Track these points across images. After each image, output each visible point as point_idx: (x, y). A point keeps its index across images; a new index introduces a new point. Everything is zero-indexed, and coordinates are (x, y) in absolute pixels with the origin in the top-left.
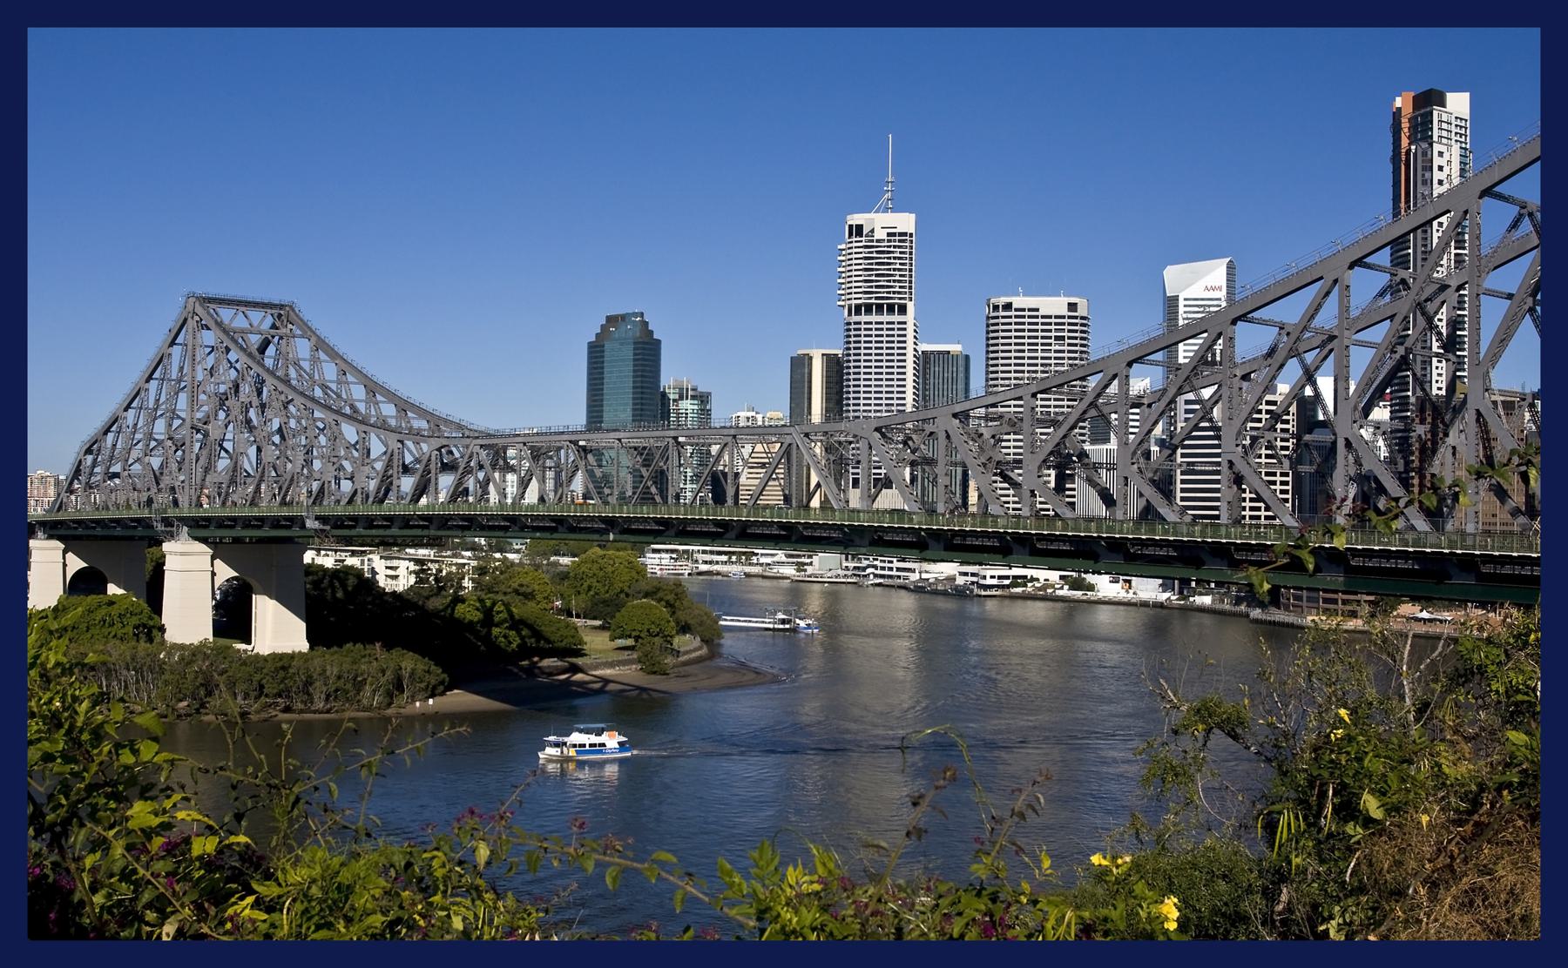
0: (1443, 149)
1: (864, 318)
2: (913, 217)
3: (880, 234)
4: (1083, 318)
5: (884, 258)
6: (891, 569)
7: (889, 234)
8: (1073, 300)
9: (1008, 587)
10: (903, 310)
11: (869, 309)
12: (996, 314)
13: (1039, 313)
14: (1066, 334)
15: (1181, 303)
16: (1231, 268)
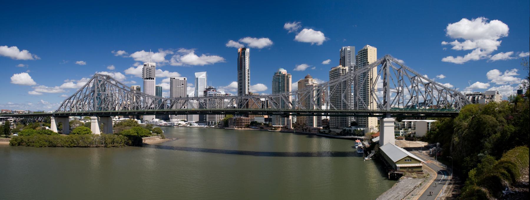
1: (147, 80)
3: (150, 66)
6: (154, 123)
8: (185, 78)
9: (178, 125)
10: (153, 79)
11: (148, 79)
13: (180, 80)
15: (199, 79)
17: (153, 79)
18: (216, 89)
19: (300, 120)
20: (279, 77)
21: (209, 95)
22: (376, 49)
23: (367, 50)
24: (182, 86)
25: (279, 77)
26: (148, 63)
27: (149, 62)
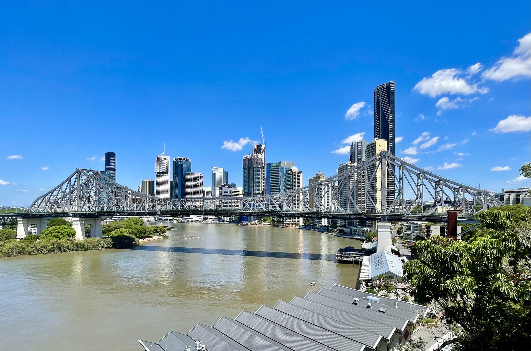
2: (169, 157)
3: (164, 160)
4: (202, 177)
7: (165, 160)
10: (167, 173)
11: (161, 173)
13: (195, 175)
14: (199, 179)
15: (216, 174)
17: (167, 173)
20: (290, 175)
21: (224, 191)
22: (387, 141)
23: (375, 143)
24: (197, 181)
25: (290, 175)
26: (161, 156)
27: (162, 155)
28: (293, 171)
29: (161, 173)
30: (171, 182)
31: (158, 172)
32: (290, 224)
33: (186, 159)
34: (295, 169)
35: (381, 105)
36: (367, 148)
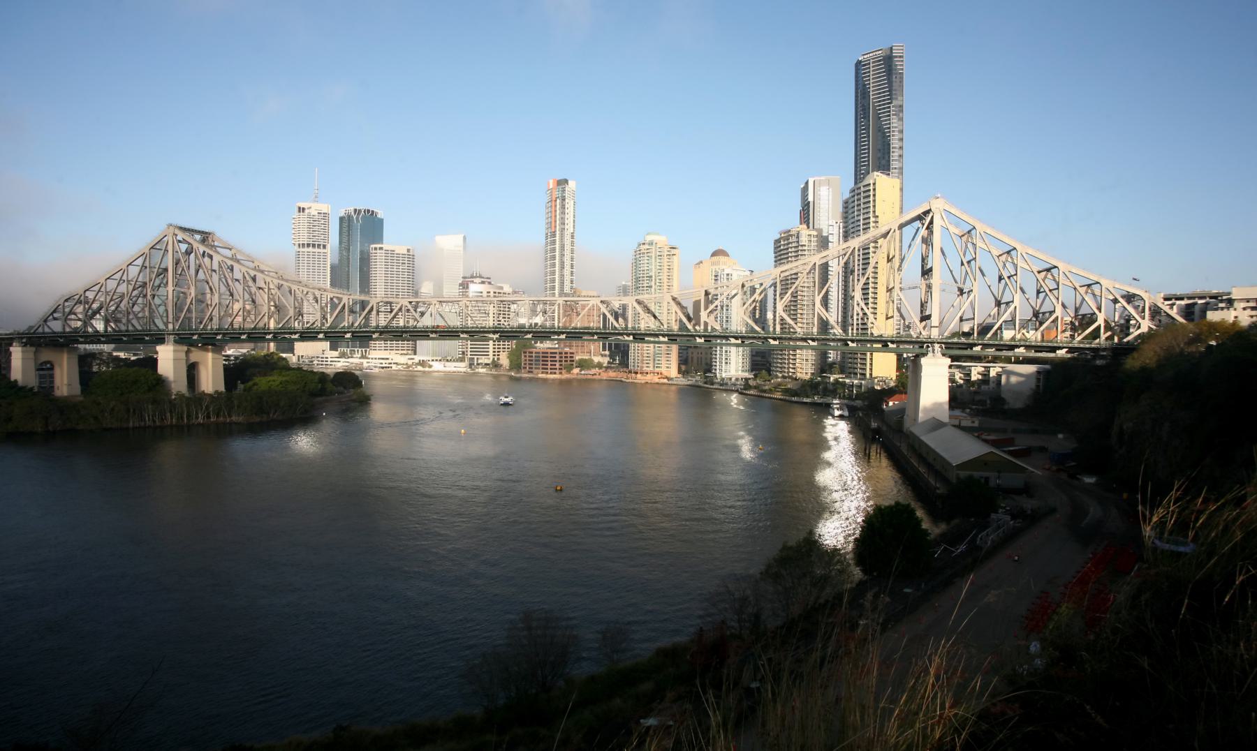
0: (569, 201)
1: (306, 249)
3: (314, 212)
4: (413, 256)
5: (316, 223)
7: (319, 213)
8: (409, 248)
10: (324, 247)
11: (308, 245)
12: (375, 252)
13: (395, 252)
16: (465, 238)
18: (490, 278)
19: (698, 358)
21: (473, 292)
28: (656, 243)
29: (308, 245)
30: (333, 268)
31: (301, 242)
32: (647, 373)
33: (373, 212)
34: (661, 239)
35: (871, 97)
36: (852, 194)
